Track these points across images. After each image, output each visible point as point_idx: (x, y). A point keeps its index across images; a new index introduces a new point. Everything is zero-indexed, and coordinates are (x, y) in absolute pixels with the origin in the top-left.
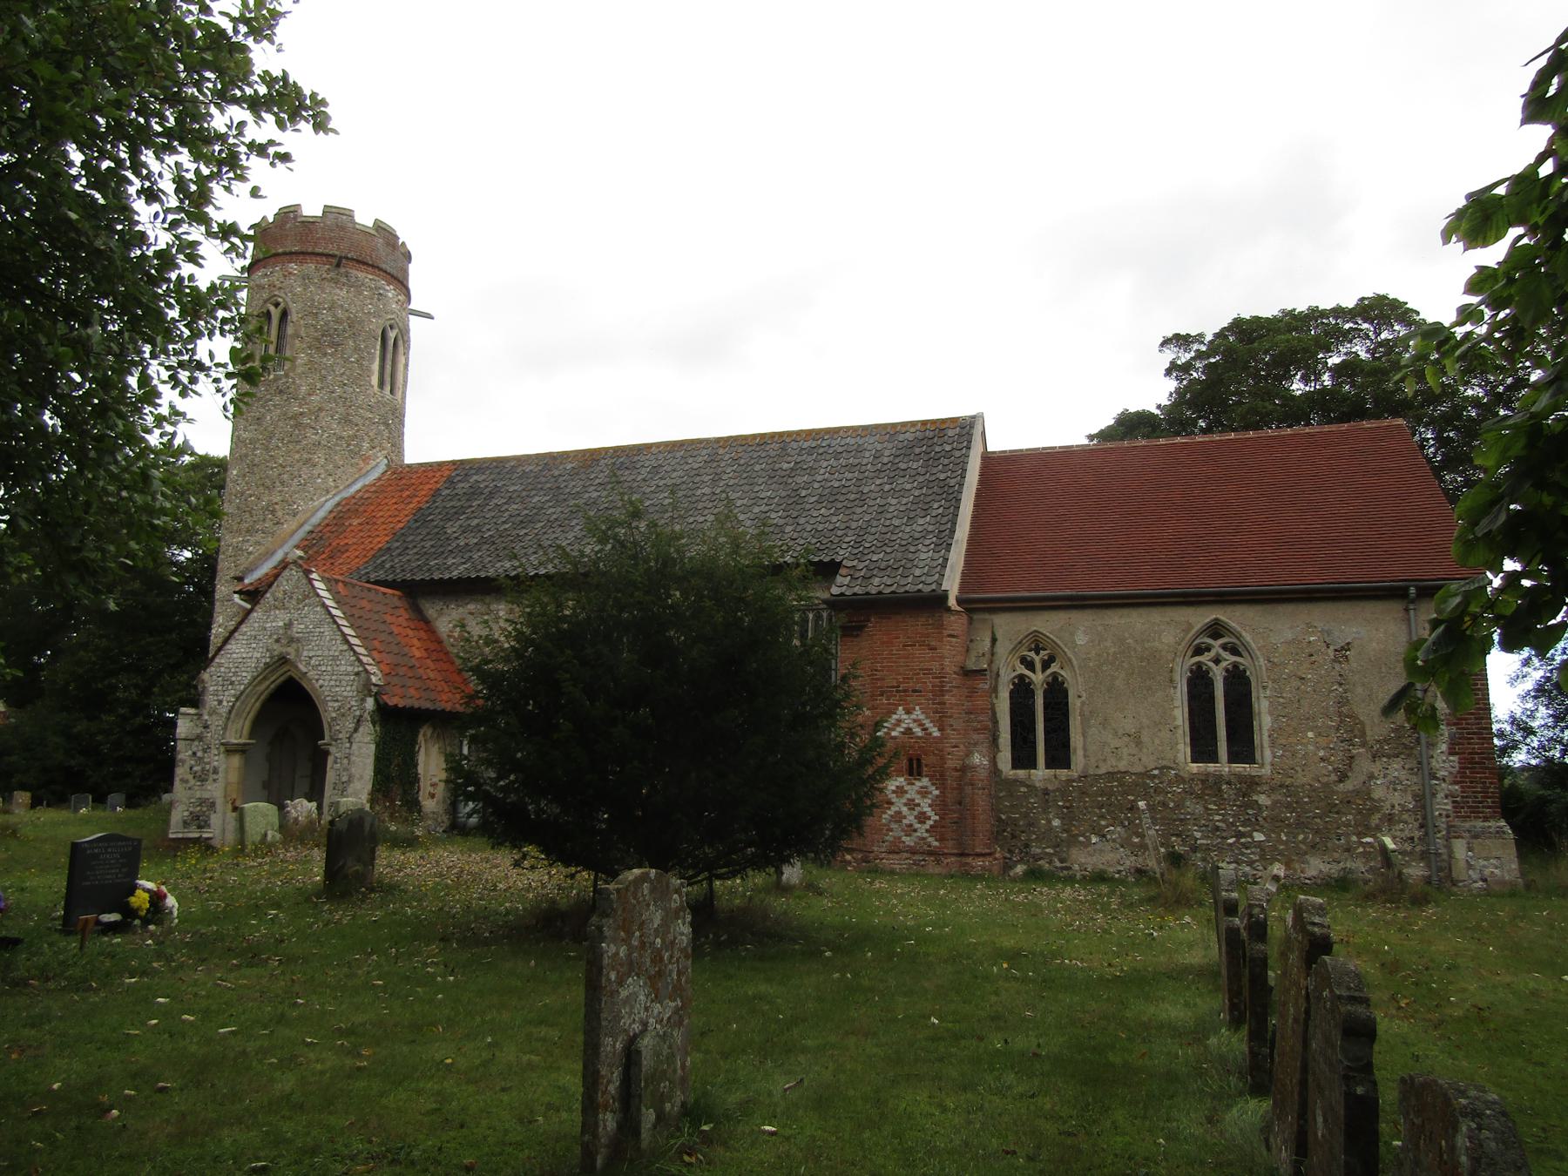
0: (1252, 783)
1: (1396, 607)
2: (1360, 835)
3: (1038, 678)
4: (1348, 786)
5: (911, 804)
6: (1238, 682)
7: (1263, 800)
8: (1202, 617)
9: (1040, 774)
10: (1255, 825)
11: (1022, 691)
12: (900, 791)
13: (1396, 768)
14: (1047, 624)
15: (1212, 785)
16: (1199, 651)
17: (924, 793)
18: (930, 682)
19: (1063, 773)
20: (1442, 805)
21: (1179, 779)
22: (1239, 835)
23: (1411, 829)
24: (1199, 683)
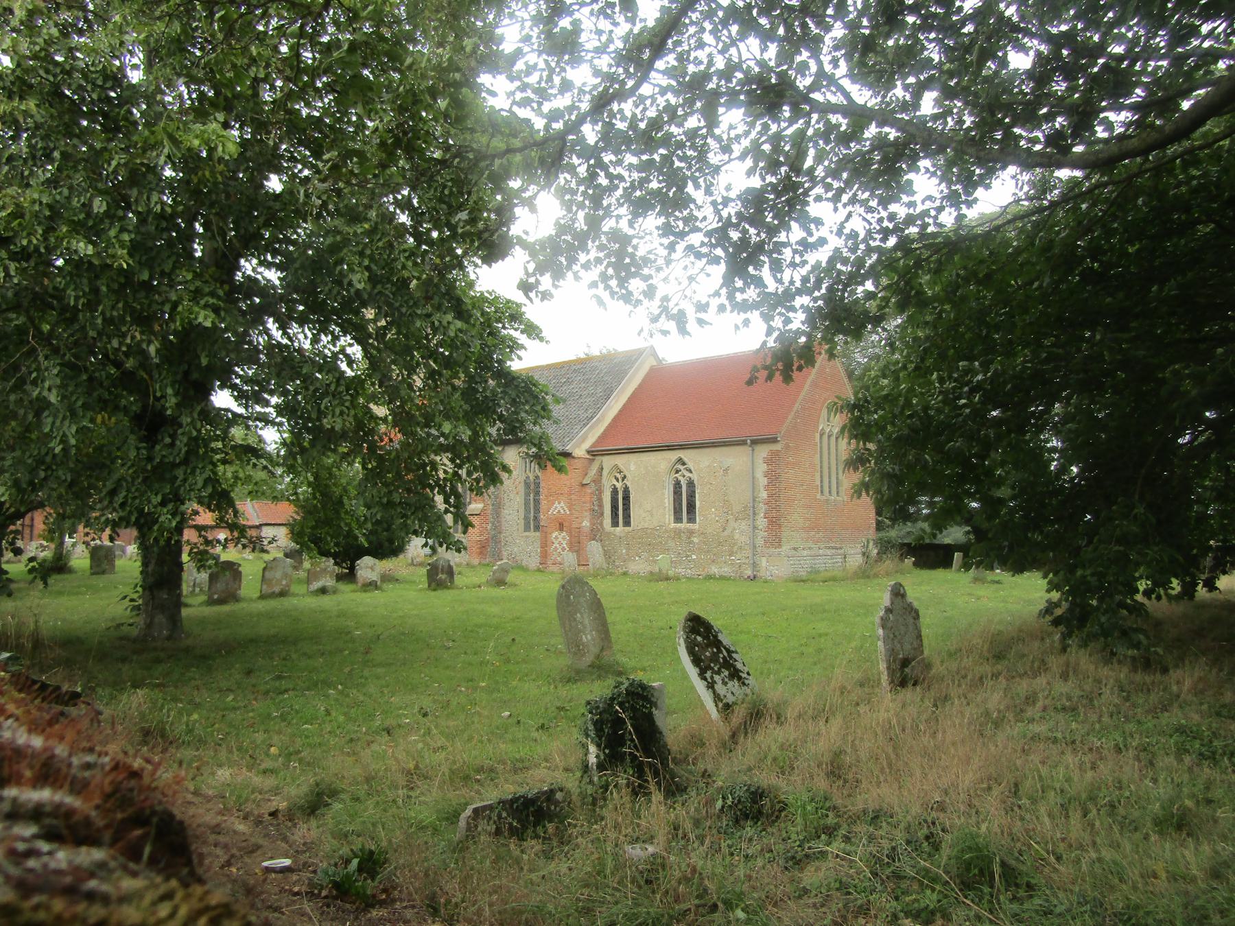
0: (691, 532)
1: (747, 449)
2: (730, 555)
3: (619, 485)
4: (726, 533)
5: (560, 544)
6: (691, 484)
7: (696, 540)
8: (674, 456)
9: (620, 529)
10: (693, 552)
11: (615, 491)
12: (556, 538)
13: (744, 525)
14: (620, 460)
15: (678, 533)
16: (677, 472)
17: (564, 538)
18: (566, 490)
19: (627, 529)
20: (760, 542)
21: (666, 531)
22: (687, 556)
23: (749, 553)
24: (677, 485)
